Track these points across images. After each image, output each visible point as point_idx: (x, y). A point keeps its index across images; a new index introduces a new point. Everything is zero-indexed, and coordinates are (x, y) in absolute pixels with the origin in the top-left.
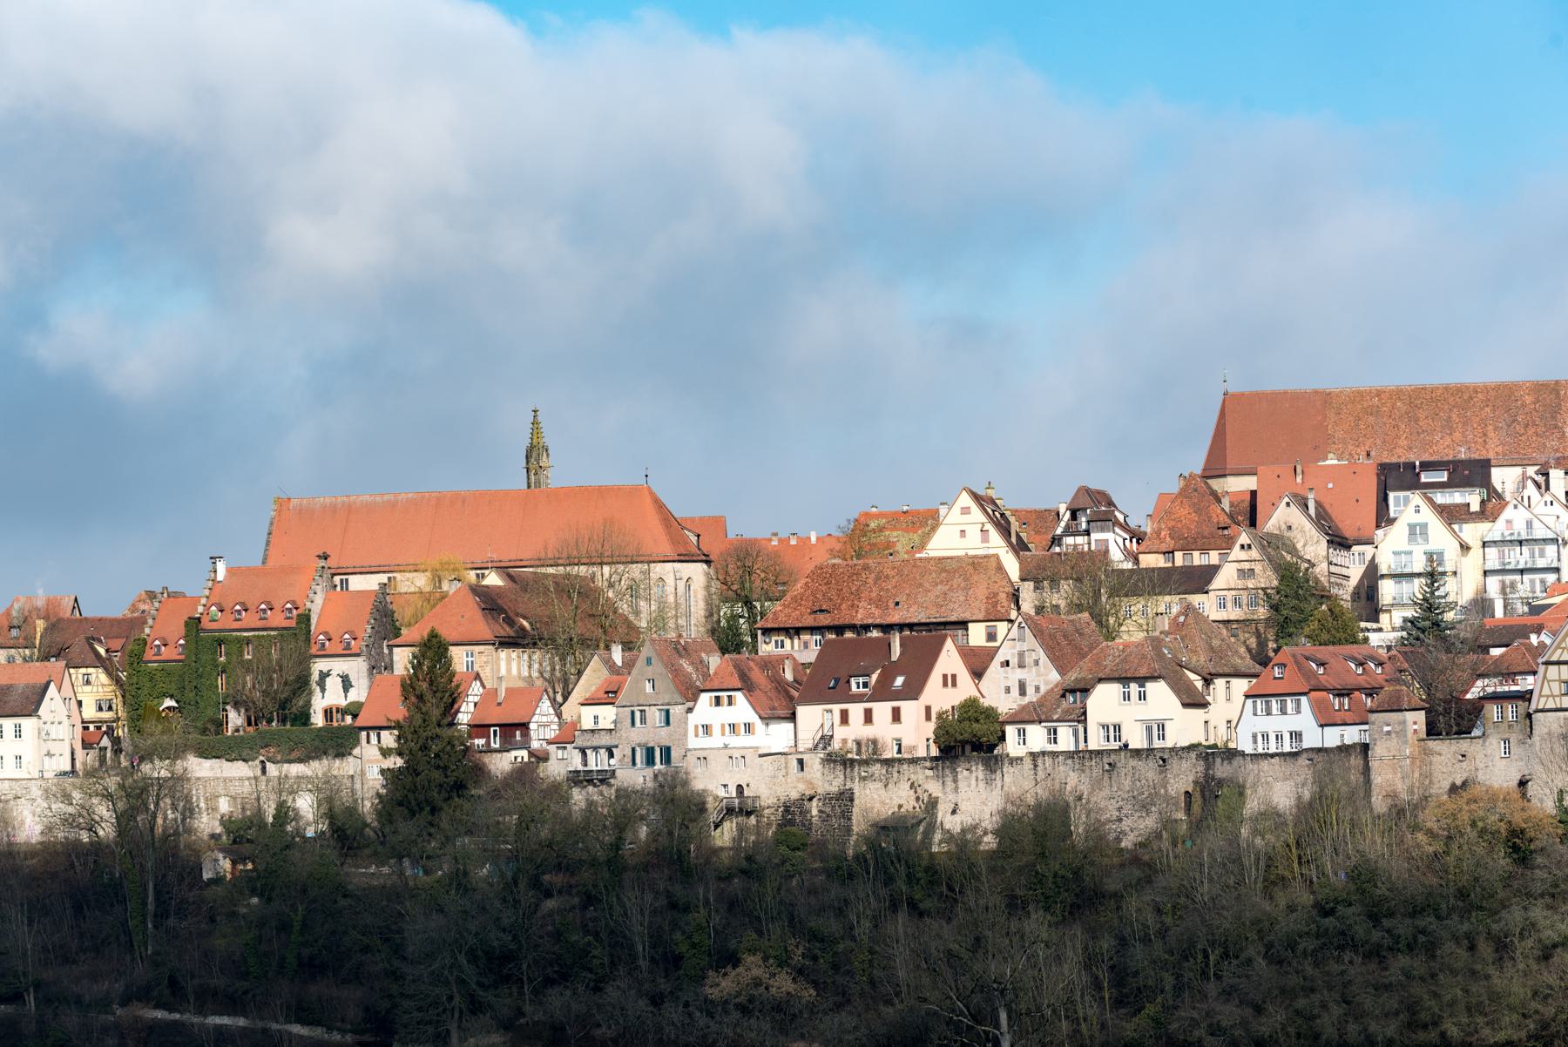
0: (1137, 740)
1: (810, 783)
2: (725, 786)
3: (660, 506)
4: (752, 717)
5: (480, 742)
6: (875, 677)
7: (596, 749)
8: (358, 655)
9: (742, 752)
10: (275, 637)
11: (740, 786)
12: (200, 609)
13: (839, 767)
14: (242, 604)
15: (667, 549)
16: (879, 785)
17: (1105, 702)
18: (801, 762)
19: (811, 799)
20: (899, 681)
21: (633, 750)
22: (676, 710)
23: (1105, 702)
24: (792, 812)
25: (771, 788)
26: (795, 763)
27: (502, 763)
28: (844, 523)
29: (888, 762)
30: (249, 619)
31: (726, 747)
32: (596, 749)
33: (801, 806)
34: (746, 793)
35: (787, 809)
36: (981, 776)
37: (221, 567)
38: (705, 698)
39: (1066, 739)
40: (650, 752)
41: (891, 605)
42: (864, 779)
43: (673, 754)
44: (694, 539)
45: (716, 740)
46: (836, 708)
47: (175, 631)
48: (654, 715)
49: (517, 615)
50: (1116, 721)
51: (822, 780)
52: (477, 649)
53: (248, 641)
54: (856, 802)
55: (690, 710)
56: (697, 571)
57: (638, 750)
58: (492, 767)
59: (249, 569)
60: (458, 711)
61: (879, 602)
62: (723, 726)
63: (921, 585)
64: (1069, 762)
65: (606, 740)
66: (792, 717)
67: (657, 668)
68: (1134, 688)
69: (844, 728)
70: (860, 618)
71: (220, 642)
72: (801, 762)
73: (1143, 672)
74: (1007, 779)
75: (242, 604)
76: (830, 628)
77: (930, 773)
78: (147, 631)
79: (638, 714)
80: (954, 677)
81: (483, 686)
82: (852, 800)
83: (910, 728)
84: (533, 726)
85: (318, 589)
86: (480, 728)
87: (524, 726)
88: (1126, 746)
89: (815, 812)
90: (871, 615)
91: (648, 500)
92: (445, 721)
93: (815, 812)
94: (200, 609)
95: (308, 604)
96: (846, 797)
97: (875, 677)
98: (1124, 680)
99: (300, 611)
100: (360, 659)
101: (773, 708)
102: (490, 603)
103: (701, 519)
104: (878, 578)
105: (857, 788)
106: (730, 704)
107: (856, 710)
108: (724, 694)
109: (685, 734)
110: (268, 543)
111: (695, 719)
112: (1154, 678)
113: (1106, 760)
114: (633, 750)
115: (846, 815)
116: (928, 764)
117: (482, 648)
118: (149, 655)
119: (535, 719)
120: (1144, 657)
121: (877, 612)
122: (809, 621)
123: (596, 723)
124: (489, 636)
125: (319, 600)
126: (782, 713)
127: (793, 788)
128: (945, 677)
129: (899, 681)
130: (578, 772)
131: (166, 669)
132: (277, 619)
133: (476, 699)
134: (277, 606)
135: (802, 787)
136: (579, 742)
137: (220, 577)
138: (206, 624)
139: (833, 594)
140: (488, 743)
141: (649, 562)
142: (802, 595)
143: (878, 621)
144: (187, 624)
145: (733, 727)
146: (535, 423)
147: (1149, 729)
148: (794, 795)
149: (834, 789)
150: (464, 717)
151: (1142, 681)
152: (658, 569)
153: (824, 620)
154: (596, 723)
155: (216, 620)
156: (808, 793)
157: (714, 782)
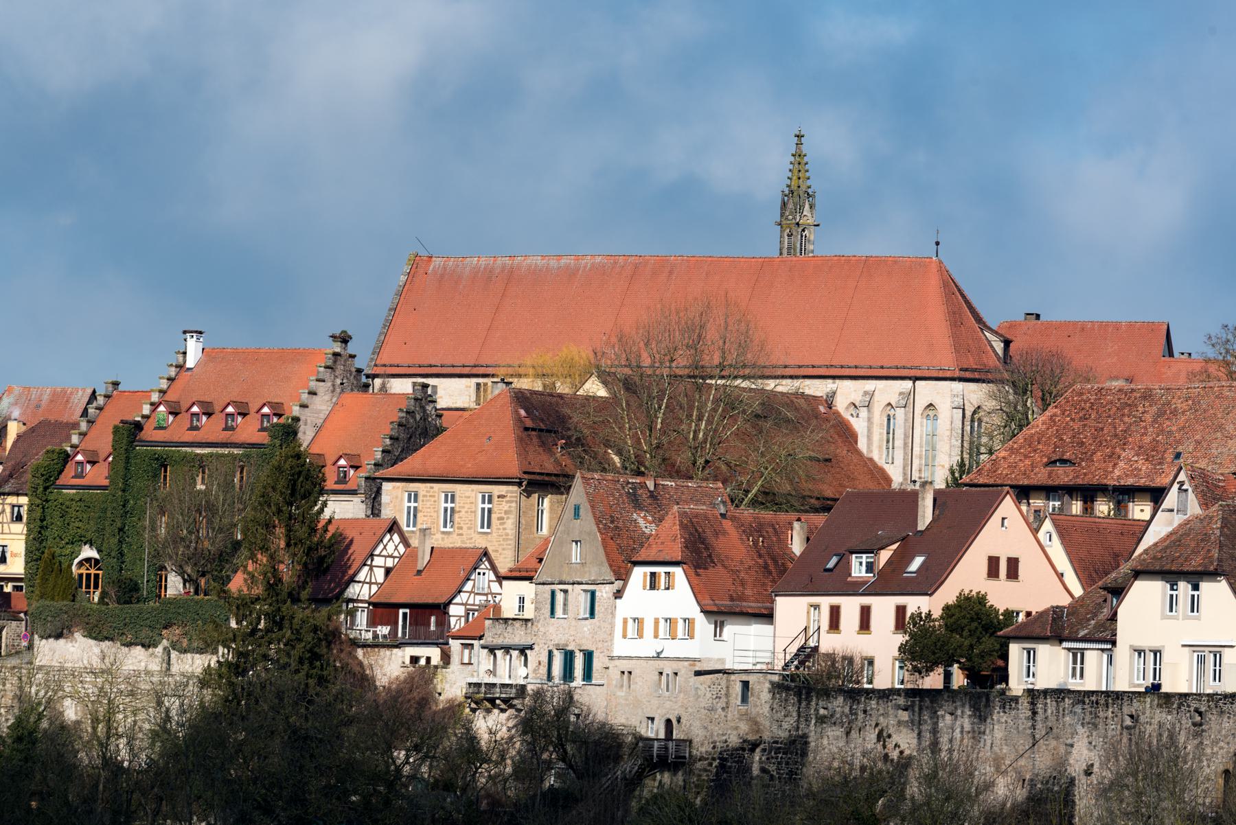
0: (1178, 679)
1: (754, 722)
2: (652, 719)
3: (953, 292)
4: (691, 608)
5: (384, 630)
6: (885, 555)
7: (507, 649)
8: (353, 492)
9: (676, 666)
10: (234, 457)
11: (669, 722)
12: (146, 410)
13: (793, 699)
14: (201, 403)
15: (948, 361)
16: (838, 732)
17: (1144, 608)
18: (746, 684)
19: (753, 750)
20: (918, 562)
21: (550, 652)
22: (604, 593)
23: (1144, 608)
24: (731, 763)
25: (709, 726)
26: (738, 688)
27: (390, 667)
28: (1216, 331)
29: (855, 695)
30: (211, 428)
31: (658, 656)
32: (507, 649)
33: (740, 760)
34: (676, 735)
35: (722, 766)
36: (967, 727)
37: (194, 349)
38: (639, 575)
39: (1095, 674)
40: (569, 657)
41: (1169, 457)
42: (821, 720)
43: (597, 664)
44: (999, 347)
45: (647, 647)
46: (826, 602)
47: (103, 441)
48: (578, 597)
49: (608, 445)
50: (1155, 644)
51: (769, 718)
52: (497, 490)
53: (201, 464)
54: (811, 757)
55: (618, 594)
56: (975, 394)
57: (556, 653)
58: (378, 674)
59: (236, 352)
60: (352, 580)
61: (1152, 453)
62: (657, 621)
63: (1221, 427)
64: (1078, 709)
65: (517, 636)
66: (767, 616)
67: (587, 522)
68: (1184, 587)
69: (833, 636)
70: (1118, 475)
71: (162, 463)
72: (746, 684)
73: (1195, 564)
74: (999, 733)
75: (201, 403)
76: (1071, 491)
77: (905, 716)
78: (75, 439)
79: (560, 597)
80: (1013, 564)
81: (405, 541)
82: (804, 754)
83: (872, 638)
84: (454, 610)
85: (322, 388)
86: (382, 610)
87: (441, 609)
88: (1156, 687)
89: (756, 770)
90: (1135, 472)
91: (934, 282)
92: (304, 595)
93: (756, 770)
94: (146, 410)
95: (296, 411)
96: (796, 747)
97: (885, 555)
98: (1171, 576)
99: (282, 420)
100: (357, 500)
101: (742, 598)
102: (544, 419)
103: (1131, 325)
104: (1161, 413)
105: (812, 730)
106: (668, 589)
107: (850, 606)
108: (660, 570)
109: (611, 634)
110: (388, 324)
111: (625, 608)
112: (1213, 575)
113: (1126, 710)
114: (550, 652)
115: (793, 776)
116: (901, 701)
117: (502, 489)
118: (67, 477)
119: (462, 597)
120: (1206, 538)
121: (1144, 467)
122: (1041, 476)
123: (521, 608)
124: (514, 470)
125: (322, 405)
126: (751, 606)
127: (731, 730)
128: (993, 562)
129: (918, 562)
130: (478, 685)
131: (87, 498)
132: (249, 431)
133: (390, 563)
134: (253, 407)
135: (744, 727)
136: (489, 639)
137: (190, 363)
138: (149, 433)
139: (1087, 437)
140: (394, 632)
141: (915, 379)
142: (1042, 434)
143: (1143, 482)
144: (116, 430)
145: (670, 621)
146: (799, 155)
147: (1201, 660)
148: (734, 741)
149: (783, 735)
150: (360, 591)
151: (1196, 577)
152: (926, 391)
153: (1064, 476)
154: (521, 608)
155: (165, 429)
156: (751, 737)
157: (619, 703)
